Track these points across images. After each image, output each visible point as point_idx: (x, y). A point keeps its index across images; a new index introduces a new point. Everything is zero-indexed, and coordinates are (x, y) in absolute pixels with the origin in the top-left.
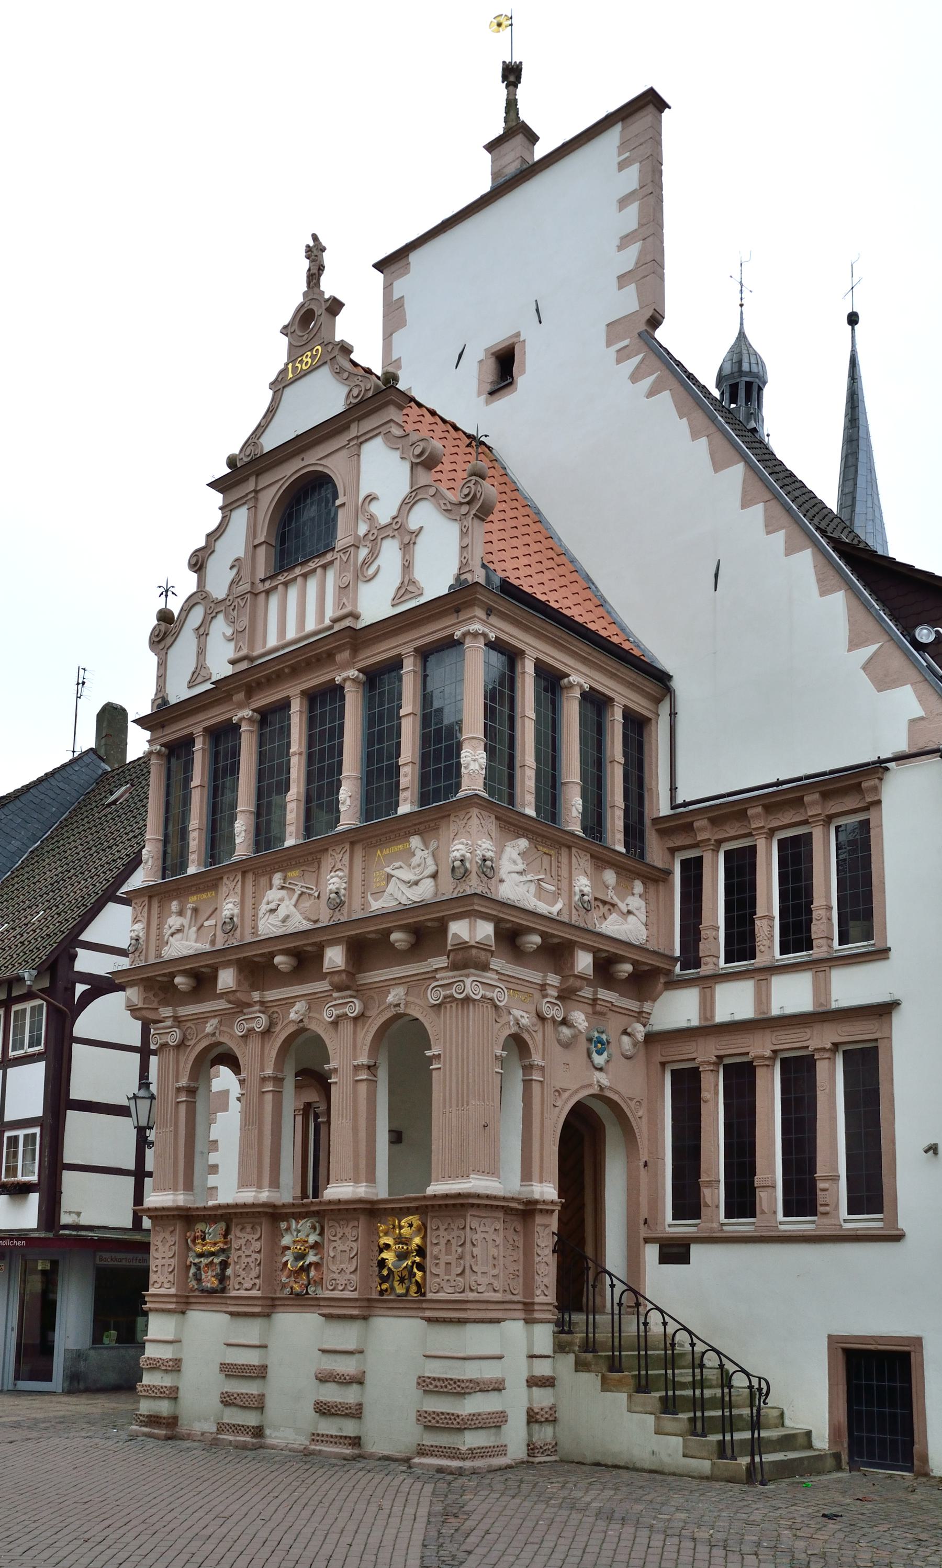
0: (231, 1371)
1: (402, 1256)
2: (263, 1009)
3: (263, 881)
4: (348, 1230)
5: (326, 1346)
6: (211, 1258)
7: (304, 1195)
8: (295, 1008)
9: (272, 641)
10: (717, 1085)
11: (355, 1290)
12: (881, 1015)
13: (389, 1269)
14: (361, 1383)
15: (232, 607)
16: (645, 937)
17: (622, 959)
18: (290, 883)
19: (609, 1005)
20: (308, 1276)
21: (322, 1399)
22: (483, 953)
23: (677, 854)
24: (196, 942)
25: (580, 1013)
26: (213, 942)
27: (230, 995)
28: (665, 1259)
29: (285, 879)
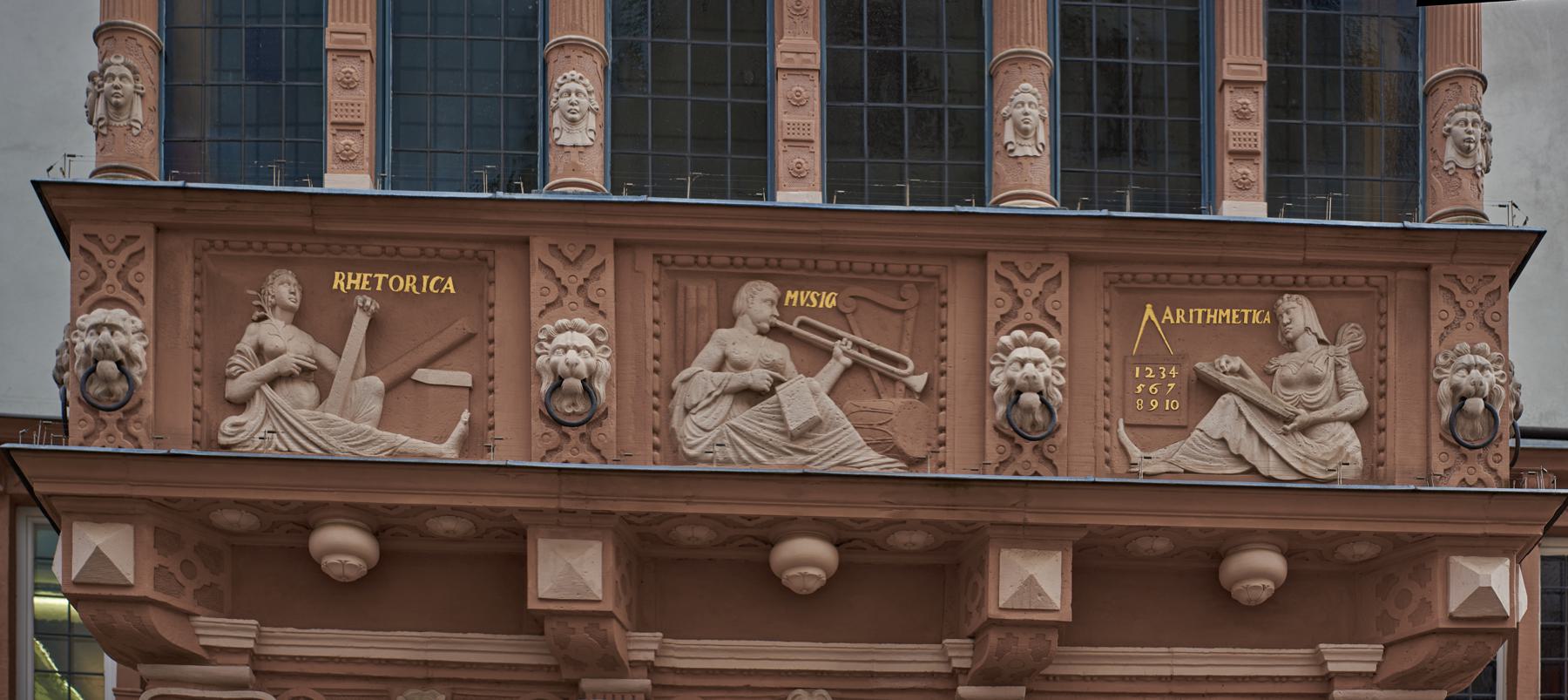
3: (700, 293)
18: (802, 324)
24: (382, 424)
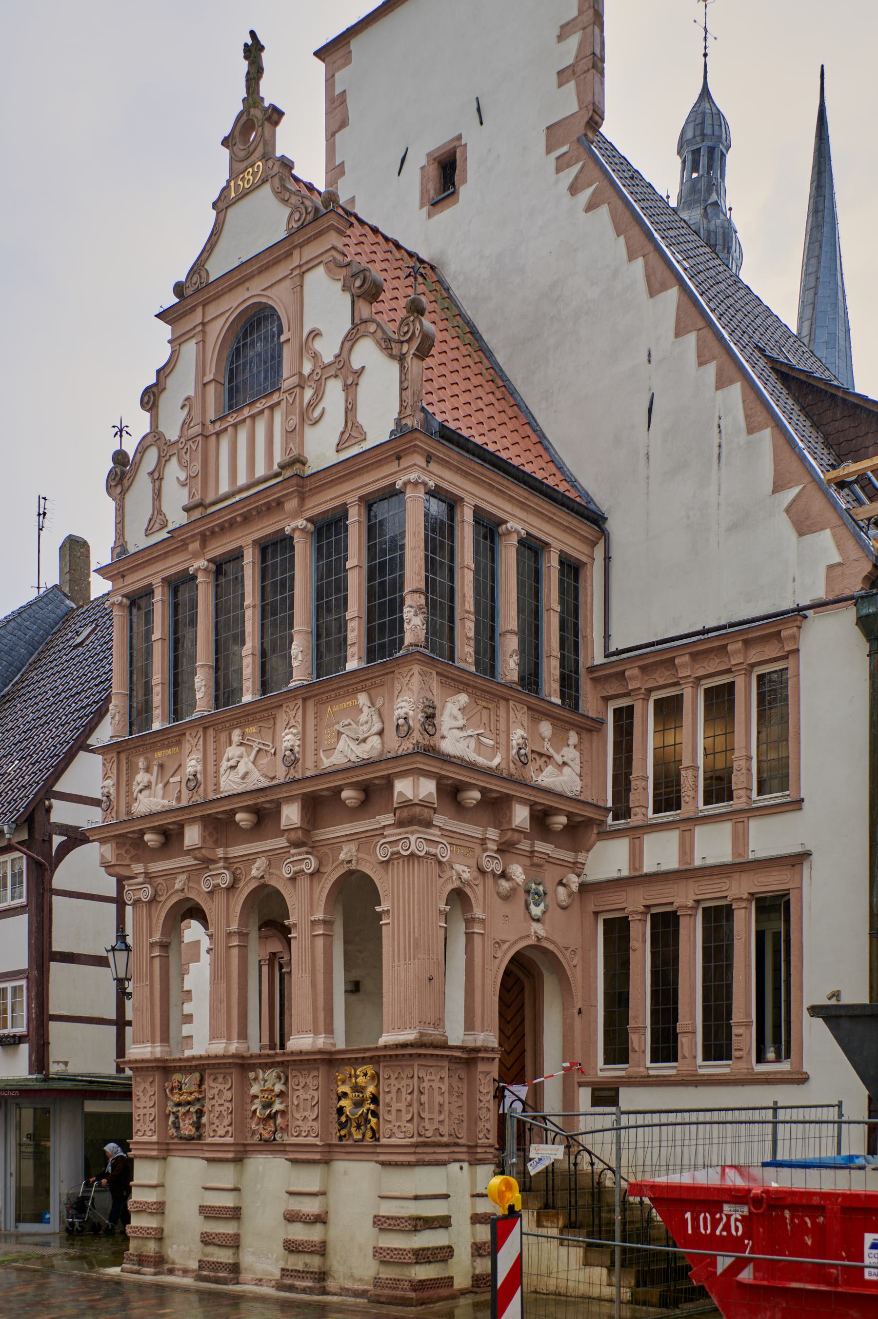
0: (209, 1213)
1: (358, 1104)
2: (227, 865)
3: (223, 736)
4: (309, 1080)
5: (293, 1189)
6: (187, 1108)
7: (272, 1046)
8: (257, 865)
9: (224, 488)
10: (644, 934)
11: (317, 1136)
12: (793, 866)
13: (347, 1116)
14: (325, 1223)
15: (185, 450)
16: (579, 789)
17: (557, 811)
19: (546, 857)
20: (275, 1123)
21: (290, 1237)
22: (426, 810)
23: (610, 703)
24: (163, 798)
25: (517, 866)
26: (179, 799)
27: (197, 852)
28: (597, 1101)
29: (243, 735)
